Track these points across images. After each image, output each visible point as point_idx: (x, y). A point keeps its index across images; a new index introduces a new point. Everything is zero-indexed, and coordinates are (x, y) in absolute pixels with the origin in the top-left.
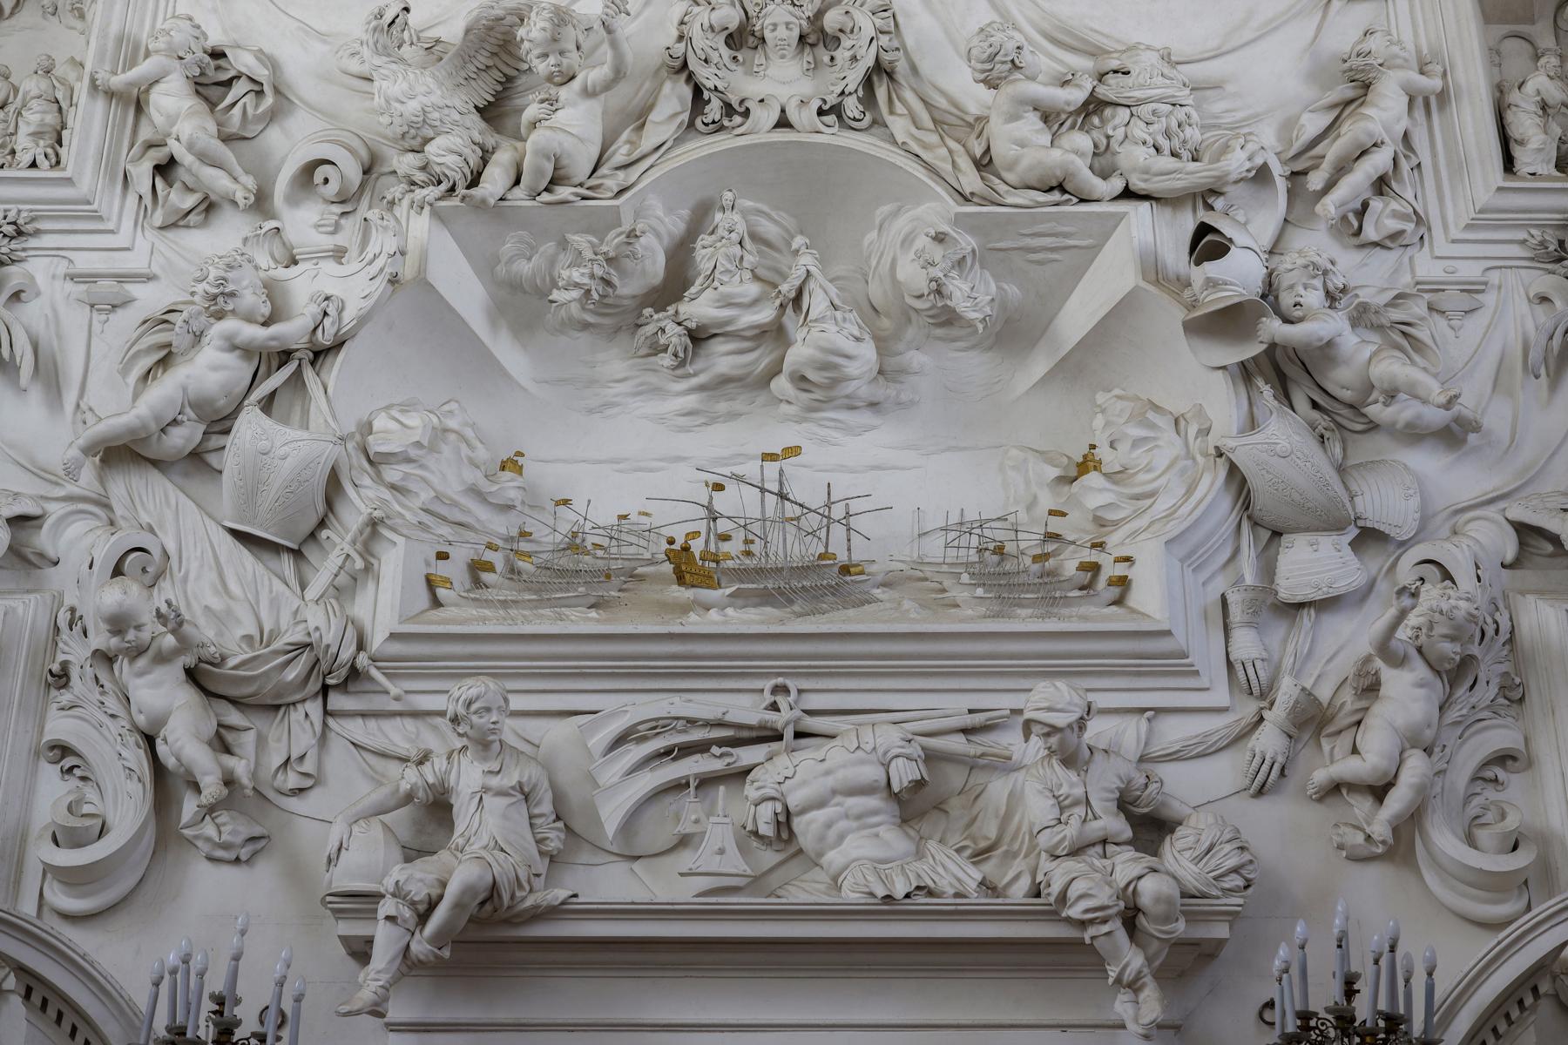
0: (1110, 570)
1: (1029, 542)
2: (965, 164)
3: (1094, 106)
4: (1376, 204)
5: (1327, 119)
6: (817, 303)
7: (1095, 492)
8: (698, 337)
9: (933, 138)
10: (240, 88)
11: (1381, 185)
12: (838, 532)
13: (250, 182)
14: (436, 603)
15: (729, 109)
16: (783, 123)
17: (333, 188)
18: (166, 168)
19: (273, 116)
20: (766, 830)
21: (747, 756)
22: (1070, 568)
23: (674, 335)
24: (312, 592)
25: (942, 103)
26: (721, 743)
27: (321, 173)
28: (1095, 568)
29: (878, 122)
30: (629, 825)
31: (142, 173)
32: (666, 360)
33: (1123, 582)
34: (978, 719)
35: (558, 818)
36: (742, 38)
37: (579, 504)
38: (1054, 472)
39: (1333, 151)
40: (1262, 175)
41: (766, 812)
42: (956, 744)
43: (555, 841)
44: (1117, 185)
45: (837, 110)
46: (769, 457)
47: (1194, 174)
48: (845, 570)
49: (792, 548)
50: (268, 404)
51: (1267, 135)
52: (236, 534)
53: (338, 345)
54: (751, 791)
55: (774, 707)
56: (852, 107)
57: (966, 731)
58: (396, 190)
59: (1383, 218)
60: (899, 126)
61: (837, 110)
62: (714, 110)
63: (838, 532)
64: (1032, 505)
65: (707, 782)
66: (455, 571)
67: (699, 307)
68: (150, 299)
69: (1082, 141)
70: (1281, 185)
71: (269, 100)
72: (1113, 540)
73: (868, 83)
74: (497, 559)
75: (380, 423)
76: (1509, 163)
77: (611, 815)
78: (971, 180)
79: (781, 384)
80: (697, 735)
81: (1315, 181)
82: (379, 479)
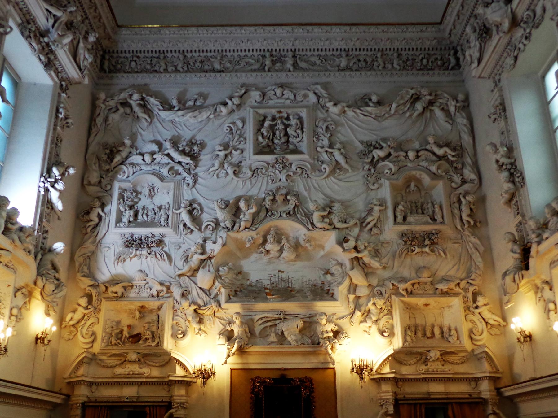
0: (331, 291)
1: (320, 283)
2: (309, 223)
3: (330, 213)
4: (373, 229)
5: (367, 213)
6: (286, 246)
7: (329, 277)
8: (268, 251)
9: (304, 218)
10: (195, 211)
11: (375, 225)
12: (290, 284)
13: (198, 227)
14: (230, 298)
15: (272, 214)
16: (281, 216)
17: (211, 229)
18: (185, 225)
19: (201, 214)
20: (280, 334)
21: (277, 322)
22: (326, 288)
23: (264, 251)
24: (212, 297)
25: (306, 210)
26: (273, 320)
27: (209, 227)
28: (329, 290)
29: (296, 214)
30: (260, 333)
31: (181, 226)
32: (263, 254)
33: (333, 294)
34: (311, 315)
35: (250, 332)
36: (274, 200)
37: (251, 280)
38: (323, 273)
39: (368, 220)
40: (356, 223)
41: (280, 331)
42: (307, 319)
43: (249, 335)
44: (333, 227)
45: (289, 213)
46: (279, 271)
47: (345, 225)
48: (291, 291)
49: (282, 285)
50: (203, 268)
51: (357, 215)
52: (200, 288)
53: (214, 257)
54: (277, 328)
55: (280, 314)
56: (291, 213)
57: (309, 317)
58: (221, 228)
59: (375, 230)
60: (299, 216)
61: (289, 213)
62: (270, 213)
63: (290, 284)
64: (320, 278)
65: (270, 326)
66: (233, 293)
67: (268, 246)
68: (184, 247)
69: (327, 220)
70: (359, 225)
71: (200, 212)
72: (331, 286)
73: (294, 208)
74: (238, 289)
75: (221, 269)
76: (395, 220)
77: (257, 333)
78: (310, 227)
79: (281, 258)
80: (270, 319)
81: (364, 224)
82: (221, 279)
